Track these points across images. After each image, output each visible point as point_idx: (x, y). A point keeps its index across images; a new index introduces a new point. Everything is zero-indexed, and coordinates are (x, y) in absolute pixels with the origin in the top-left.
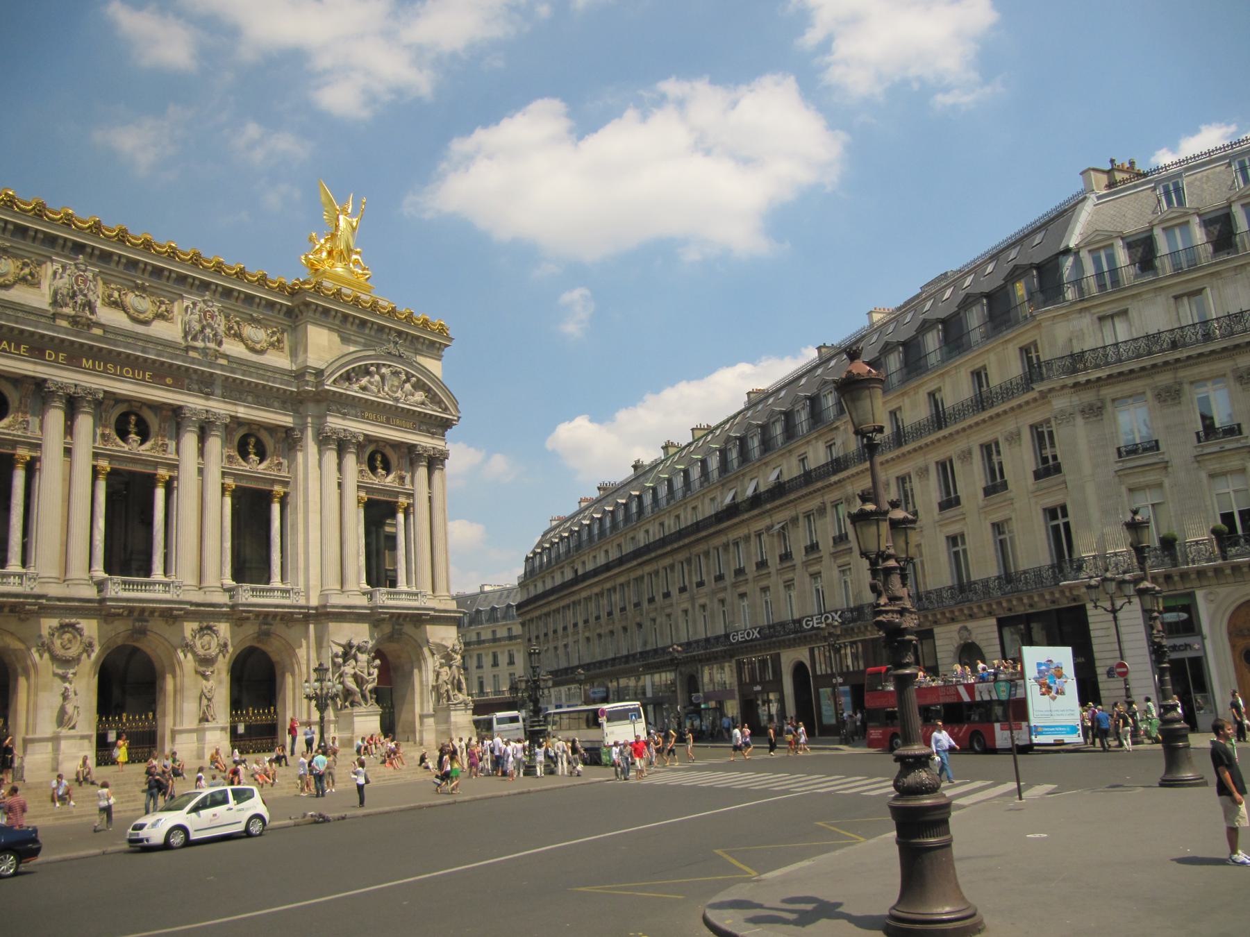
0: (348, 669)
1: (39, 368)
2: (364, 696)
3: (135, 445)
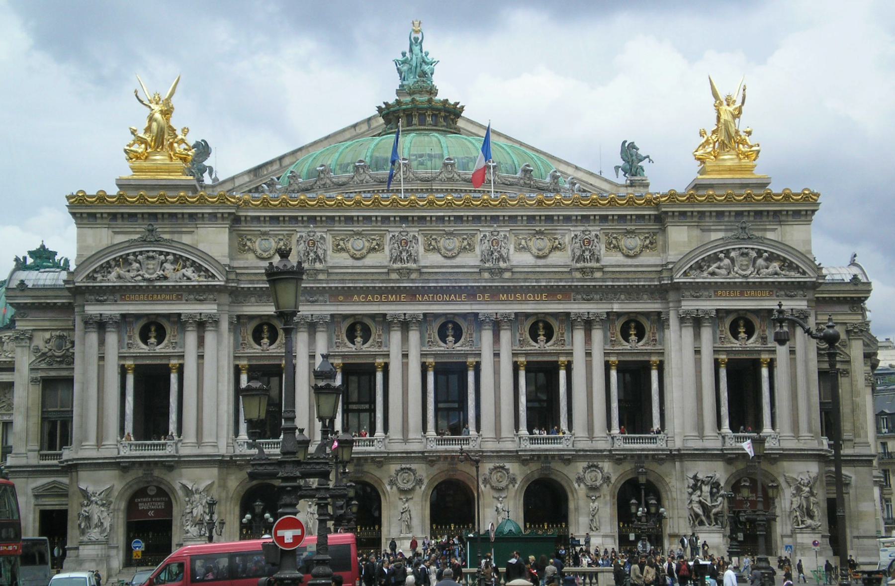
0: (695, 498)
1: (474, 307)
2: (708, 517)
3: (542, 343)
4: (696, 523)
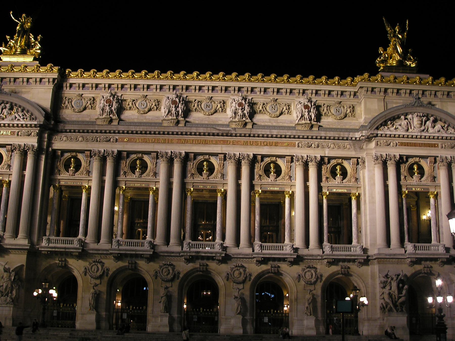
2: (395, 306)
4: (387, 310)
